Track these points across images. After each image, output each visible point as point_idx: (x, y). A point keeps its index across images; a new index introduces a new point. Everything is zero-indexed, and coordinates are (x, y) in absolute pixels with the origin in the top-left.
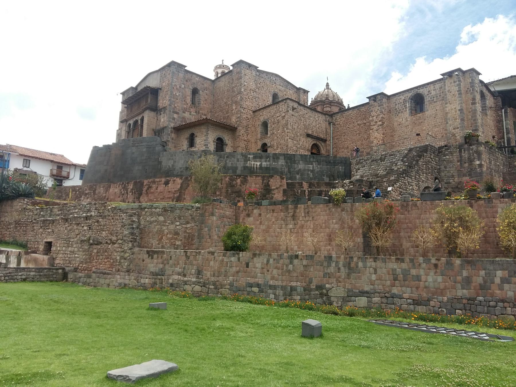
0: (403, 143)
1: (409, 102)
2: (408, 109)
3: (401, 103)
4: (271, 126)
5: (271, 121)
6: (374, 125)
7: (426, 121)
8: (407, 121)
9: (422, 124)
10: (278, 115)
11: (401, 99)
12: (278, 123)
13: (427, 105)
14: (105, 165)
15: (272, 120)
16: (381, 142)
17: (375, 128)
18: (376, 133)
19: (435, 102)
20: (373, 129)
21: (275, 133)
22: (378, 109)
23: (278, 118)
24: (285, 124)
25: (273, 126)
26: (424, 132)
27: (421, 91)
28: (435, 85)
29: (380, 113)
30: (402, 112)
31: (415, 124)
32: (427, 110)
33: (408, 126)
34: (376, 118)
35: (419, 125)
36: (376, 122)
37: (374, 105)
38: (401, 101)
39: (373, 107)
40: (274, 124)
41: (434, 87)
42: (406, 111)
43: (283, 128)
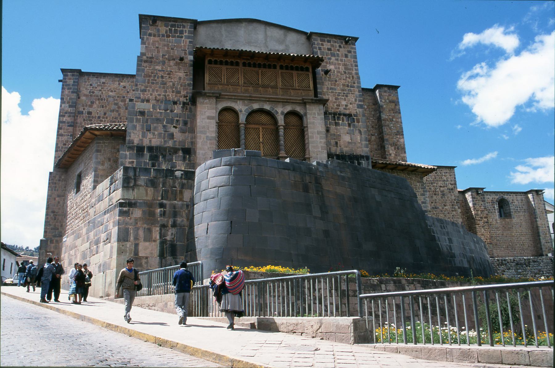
0: (496, 245)
1: (496, 204)
2: (496, 211)
3: (489, 203)
4: (432, 197)
5: (430, 189)
6: (480, 220)
7: (513, 227)
8: (497, 223)
9: (511, 229)
10: (440, 184)
11: (489, 198)
12: (443, 195)
13: (512, 212)
14: (315, 217)
15: (433, 188)
16: (488, 240)
17: (481, 223)
18: (483, 230)
19: (519, 212)
20: (479, 224)
21: (440, 208)
22: (482, 205)
23: (442, 189)
24: (455, 200)
25: (435, 197)
26: (514, 238)
27: (506, 197)
28: (517, 196)
29: (485, 209)
30: (491, 212)
31: (505, 228)
32: (514, 218)
33: (499, 228)
34: (481, 213)
35: (508, 230)
36: (482, 218)
37: (477, 198)
38: (490, 200)
39: (476, 200)
40: (435, 194)
41: (517, 198)
42: (495, 213)
43: (453, 205)
